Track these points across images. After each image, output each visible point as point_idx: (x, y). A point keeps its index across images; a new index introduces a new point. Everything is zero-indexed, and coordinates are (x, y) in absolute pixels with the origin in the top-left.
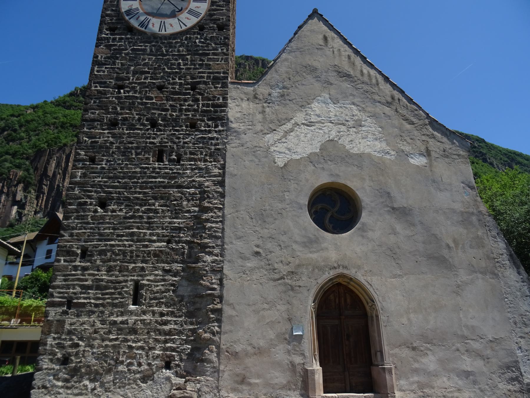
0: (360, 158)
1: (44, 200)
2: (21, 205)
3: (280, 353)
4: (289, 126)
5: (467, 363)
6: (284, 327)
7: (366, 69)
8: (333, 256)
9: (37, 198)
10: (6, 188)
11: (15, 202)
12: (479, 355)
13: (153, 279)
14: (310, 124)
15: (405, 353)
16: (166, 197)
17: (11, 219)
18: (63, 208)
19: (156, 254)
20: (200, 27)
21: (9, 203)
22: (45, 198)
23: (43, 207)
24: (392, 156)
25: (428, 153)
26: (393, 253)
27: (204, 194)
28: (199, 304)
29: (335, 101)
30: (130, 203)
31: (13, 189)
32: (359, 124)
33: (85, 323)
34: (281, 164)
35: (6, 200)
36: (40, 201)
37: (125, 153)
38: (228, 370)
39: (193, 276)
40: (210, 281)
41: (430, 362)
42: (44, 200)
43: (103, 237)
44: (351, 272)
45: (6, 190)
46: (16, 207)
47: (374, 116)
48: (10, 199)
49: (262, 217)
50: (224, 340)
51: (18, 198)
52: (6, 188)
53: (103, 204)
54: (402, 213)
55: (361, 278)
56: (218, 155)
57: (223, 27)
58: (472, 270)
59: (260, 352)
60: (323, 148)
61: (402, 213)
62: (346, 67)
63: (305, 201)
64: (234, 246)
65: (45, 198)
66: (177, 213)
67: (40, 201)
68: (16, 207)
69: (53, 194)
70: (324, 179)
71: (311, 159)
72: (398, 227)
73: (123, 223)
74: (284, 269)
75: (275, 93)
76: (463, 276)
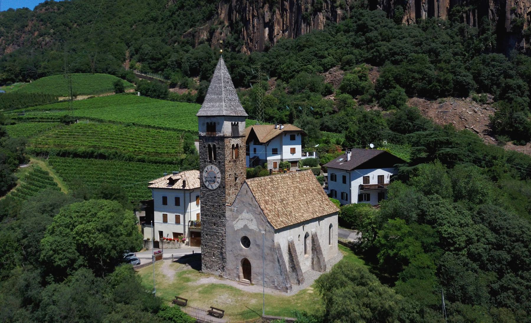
0: (251, 230)
1: (288, 17)
2: (270, 25)
3: (235, 271)
4: (237, 220)
5: (266, 279)
6: (235, 266)
7: (255, 203)
8: (244, 254)
9: (282, 16)
10: (255, 11)
11: (266, 25)
12: (268, 278)
13: (216, 252)
14: (242, 219)
15: (255, 275)
16: (216, 235)
17: (266, 42)
18: (304, 23)
19: (216, 247)
20: (219, 187)
21: (262, 25)
22: (288, 14)
23: (288, 24)
24: (258, 230)
25: (265, 230)
26: (255, 255)
27: (222, 236)
28: (223, 259)
29: (248, 213)
30: (211, 236)
31: (261, 10)
32: (252, 220)
33: (207, 259)
34: (236, 229)
35: (258, 23)
36: (285, 19)
37: (209, 223)
38: (227, 272)
39: (222, 253)
40: (224, 255)
41: (259, 278)
42: (288, 17)
43: (208, 243)
44: (247, 258)
45: (256, 13)
46: (267, 29)
47: (255, 218)
48: (261, 21)
49: (232, 243)
50: (227, 267)
51: (267, 20)
52: (255, 11)
53: (207, 235)
54: (258, 246)
55: (249, 259)
56: (224, 226)
57: (224, 187)
58: (270, 261)
59: (232, 270)
60: (244, 226)
61: (258, 246)
62: (251, 203)
63: (240, 240)
64: (228, 249)
65: (288, 14)
66: (218, 239)
67: (285, 19)
68: (267, 29)
69: (294, 10)
70: (244, 235)
71: (242, 229)
72: (257, 249)
73: (210, 240)
74: (236, 255)
75: (236, 209)
76: (268, 262)
